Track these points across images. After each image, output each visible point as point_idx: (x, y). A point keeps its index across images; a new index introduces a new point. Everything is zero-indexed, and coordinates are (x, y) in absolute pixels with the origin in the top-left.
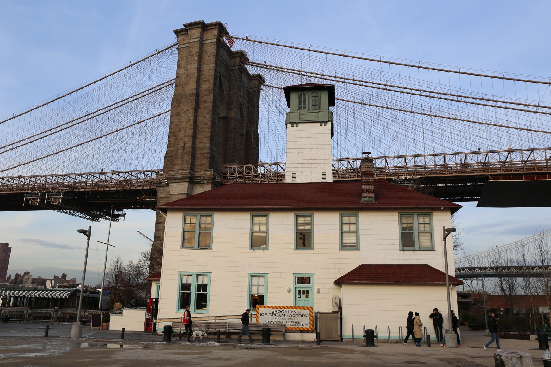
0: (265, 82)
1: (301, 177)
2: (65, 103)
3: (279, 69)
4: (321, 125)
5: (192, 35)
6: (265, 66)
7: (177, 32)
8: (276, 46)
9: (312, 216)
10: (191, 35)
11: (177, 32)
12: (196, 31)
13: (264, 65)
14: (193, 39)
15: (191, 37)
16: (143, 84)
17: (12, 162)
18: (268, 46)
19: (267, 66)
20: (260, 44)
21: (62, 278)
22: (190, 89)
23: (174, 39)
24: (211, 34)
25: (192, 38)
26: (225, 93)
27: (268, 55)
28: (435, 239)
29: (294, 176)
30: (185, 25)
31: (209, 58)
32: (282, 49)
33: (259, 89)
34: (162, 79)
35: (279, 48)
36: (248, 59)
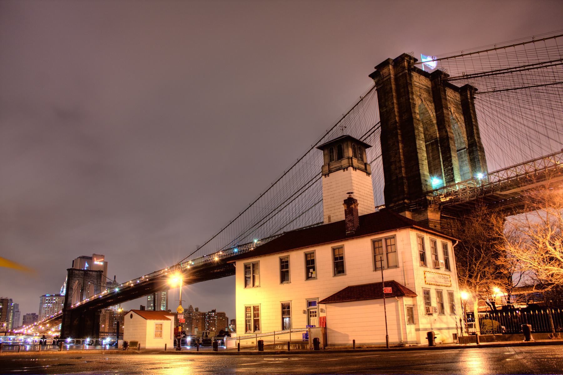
0: (477, 90)
1: (335, 218)
2: (304, 163)
3: (486, 74)
4: (326, 177)
5: (384, 74)
6: (467, 77)
7: (372, 76)
8: (461, 57)
9: (395, 238)
10: (383, 74)
11: (372, 76)
12: (386, 69)
13: (463, 76)
14: (385, 77)
15: (383, 76)
16: (362, 128)
17: (271, 222)
18: (455, 60)
19: (467, 75)
20: (446, 60)
21: (168, 310)
22: (392, 124)
23: (372, 83)
24: (401, 68)
25: (385, 76)
26: (432, 116)
27: (457, 69)
28: (317, 262)
29: (329, 218)
30: (375, 68)
31: (403, 90)
32: (469, 58)
33: (473, 98)
34: (374, 121)
35: (466, 58)
36: (448, 75)
